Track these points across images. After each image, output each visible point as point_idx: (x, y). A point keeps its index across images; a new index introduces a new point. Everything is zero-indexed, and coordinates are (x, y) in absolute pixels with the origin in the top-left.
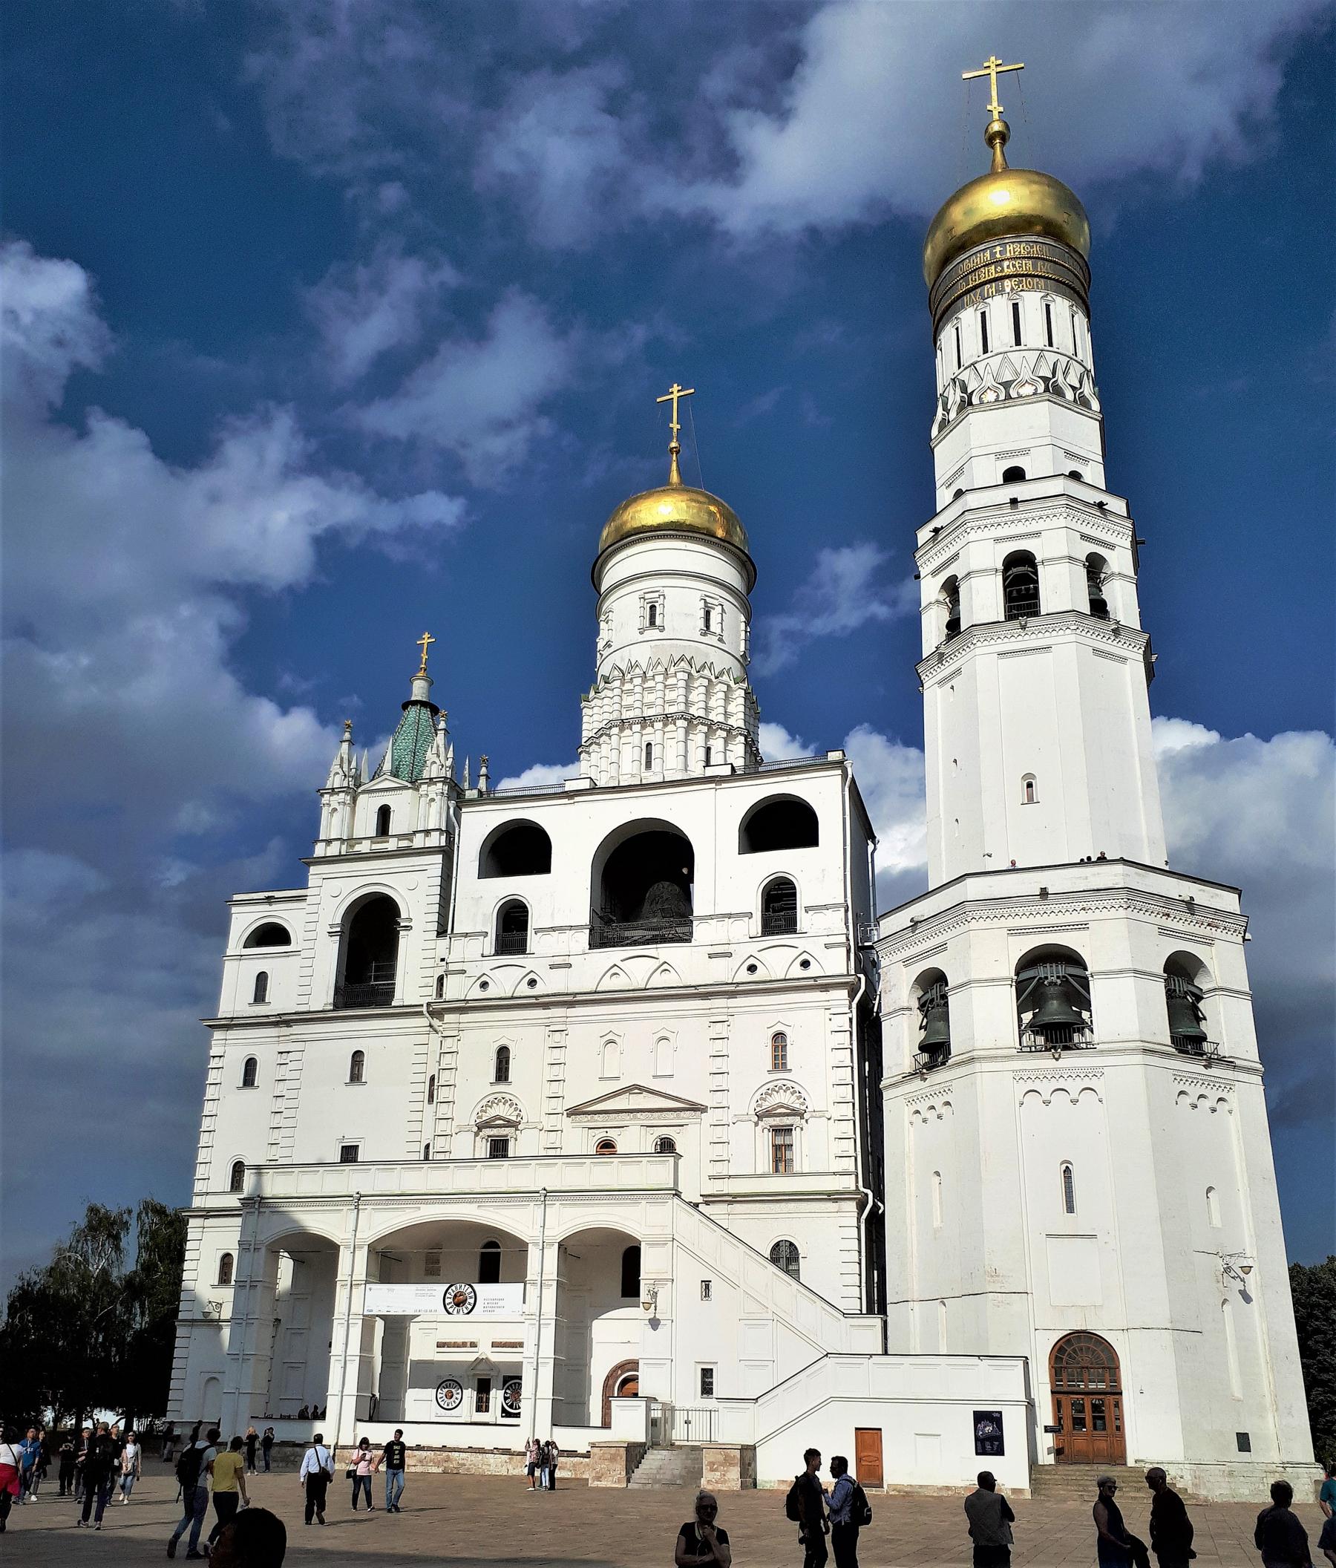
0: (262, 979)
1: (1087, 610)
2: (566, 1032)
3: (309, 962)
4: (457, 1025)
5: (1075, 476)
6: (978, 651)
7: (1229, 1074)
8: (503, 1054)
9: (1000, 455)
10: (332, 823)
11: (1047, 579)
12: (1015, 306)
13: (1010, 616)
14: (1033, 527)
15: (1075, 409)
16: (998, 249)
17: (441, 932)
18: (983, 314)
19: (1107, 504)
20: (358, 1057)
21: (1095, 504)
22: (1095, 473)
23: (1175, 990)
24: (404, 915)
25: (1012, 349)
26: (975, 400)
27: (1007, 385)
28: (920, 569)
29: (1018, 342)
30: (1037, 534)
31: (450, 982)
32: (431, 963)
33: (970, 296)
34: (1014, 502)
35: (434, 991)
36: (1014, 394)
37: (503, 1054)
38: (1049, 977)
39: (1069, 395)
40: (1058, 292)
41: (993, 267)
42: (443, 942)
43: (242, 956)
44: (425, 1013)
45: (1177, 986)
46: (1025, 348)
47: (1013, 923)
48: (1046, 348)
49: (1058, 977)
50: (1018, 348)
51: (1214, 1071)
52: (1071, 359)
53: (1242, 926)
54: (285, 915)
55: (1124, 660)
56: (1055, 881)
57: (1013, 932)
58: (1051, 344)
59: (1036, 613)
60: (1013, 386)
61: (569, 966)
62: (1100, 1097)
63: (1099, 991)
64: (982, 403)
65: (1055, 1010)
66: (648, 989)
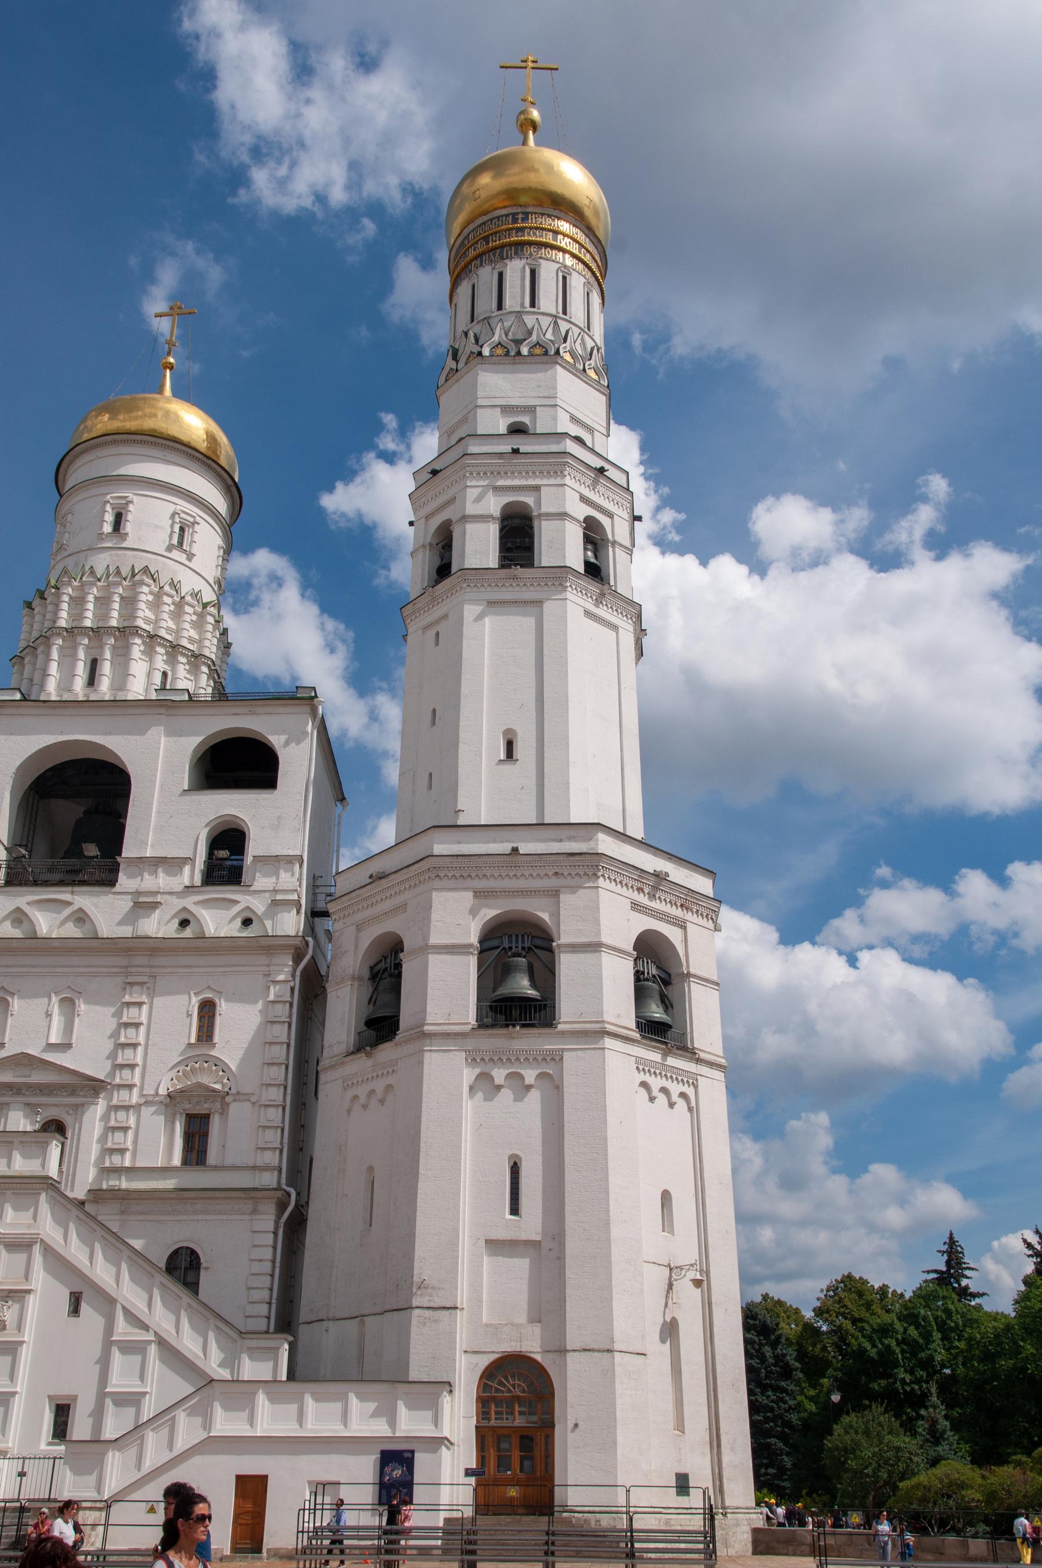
1: (581, 569)
5: (579, 440)
9: (506, 409)
11: (545, 533)
13: (502, 566)
16: (520, 216)
21: (596, 469)
23: (643, 973)
26: (486, 352)
29: (533, 304)
33: (489, 256)
34: (516, 451)
36: (525, 351)
38: (514, 947)
47: (479, 884)
50: (532, 310)
52: (584, 331)
55: (615, 628)
58: (565, 312)
62: (557, 1082)
63: (567, 966)
64: (491, 355)
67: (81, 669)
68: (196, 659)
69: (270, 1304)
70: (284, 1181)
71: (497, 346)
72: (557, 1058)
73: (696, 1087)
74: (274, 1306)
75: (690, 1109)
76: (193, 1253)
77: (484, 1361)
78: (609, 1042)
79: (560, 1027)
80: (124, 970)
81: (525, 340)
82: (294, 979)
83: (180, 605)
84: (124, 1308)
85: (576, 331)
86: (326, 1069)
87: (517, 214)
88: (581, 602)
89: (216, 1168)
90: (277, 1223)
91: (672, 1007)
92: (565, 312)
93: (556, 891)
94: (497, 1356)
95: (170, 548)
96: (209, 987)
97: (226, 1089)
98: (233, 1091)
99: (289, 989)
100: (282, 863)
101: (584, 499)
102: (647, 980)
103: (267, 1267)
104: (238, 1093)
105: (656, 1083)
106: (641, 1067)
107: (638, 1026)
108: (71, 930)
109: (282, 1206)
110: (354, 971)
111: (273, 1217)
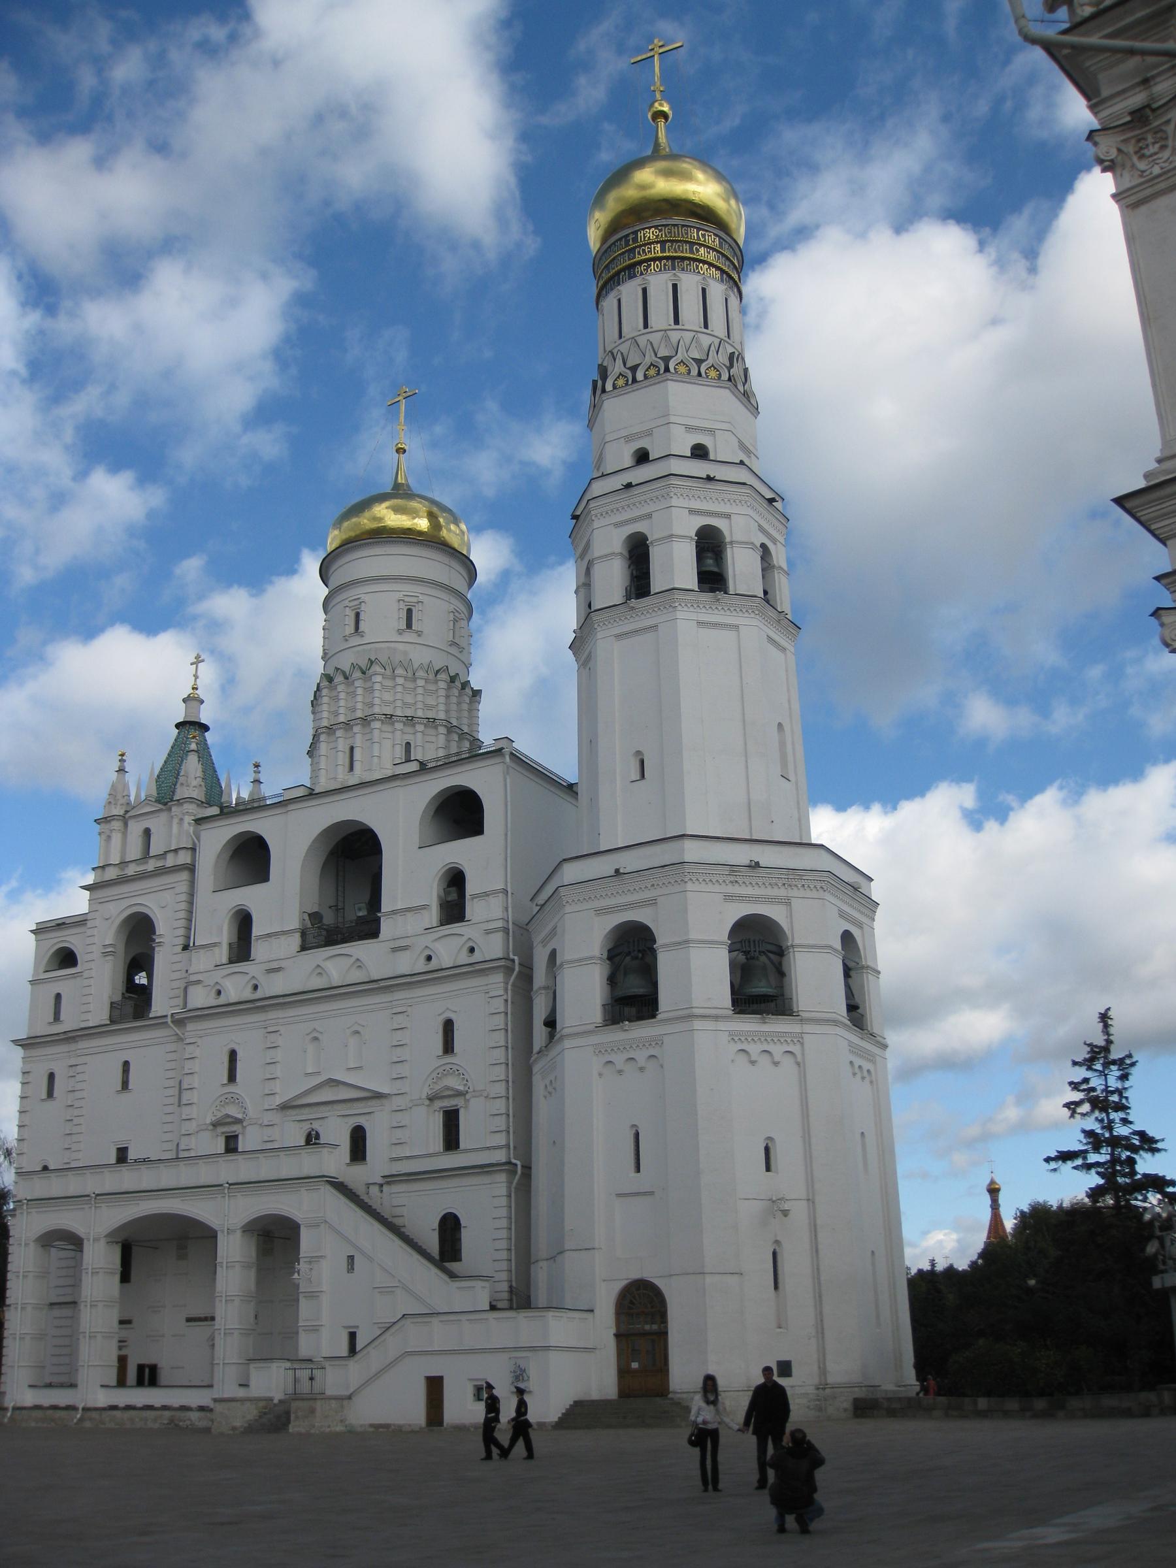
2: (279, 1033)
3: (86, 982)
6: (599, 635)
8: (233, 1055)
9: (629, 439)
12: (645, 291)
15: (700, 382)
16: (631, 237)
17: (186, 948)
18: (619, 300)
19: (715, 477)
20: (126, 1064)
25: (640, 333)
26: (609, 387)
29: (646, 326)
31: (191, 989)
32: (177, 975)
34: (629, 486)
35: (180, 1001)
36: (640, 376)
37: (233, 1055)
41: (627, 254)
42: (186, 954)
44: (170, 1023)
45: (752, 947)
48: (670, 327)
49: (639, 951)
50: (647, 330)
51: (778, 1025)
54: (73, 940)
56: (629, 862)
57: (600, 912)
58: (677, 321)
60: (639, 369)
61: (278, 970)
63: (665, 964)
65: (634, 985)
67: (343, 759)
68: (431, 722)
69: (509, 1250)
70: (512, 1156)
71: (618, 377)
72: (660, 1043)
73: (802, 1044)
74: (513, 1252)
75: (798, 1064)
77: (618, 1286)
78: (698, 1024)
79: (659, 1017)
80: (389, 1004)
82: (507, 993)
83: (414, 679)
84: (380, 1265)
85: (691, 335)
86: (535, 1060)
87: (627, 235)
89: (467, 1151)
90: (509, 1188)
91: (785, 975)
92: (677, 321)
93: (655, 900)
94: (625, 1282)
95: (400, 632)
96: (448, 1009)
97: (467, 1089)
98: (471, 1090)
100: (490, 896)
101: (692, 512)
102: (753, 958)
103: (504, 1223)
104: (474, 1091)
105: (754, 1049)
106: (736, 1039)
107: (735, 1002)
108: (356, 976)
111: (505, 1185)
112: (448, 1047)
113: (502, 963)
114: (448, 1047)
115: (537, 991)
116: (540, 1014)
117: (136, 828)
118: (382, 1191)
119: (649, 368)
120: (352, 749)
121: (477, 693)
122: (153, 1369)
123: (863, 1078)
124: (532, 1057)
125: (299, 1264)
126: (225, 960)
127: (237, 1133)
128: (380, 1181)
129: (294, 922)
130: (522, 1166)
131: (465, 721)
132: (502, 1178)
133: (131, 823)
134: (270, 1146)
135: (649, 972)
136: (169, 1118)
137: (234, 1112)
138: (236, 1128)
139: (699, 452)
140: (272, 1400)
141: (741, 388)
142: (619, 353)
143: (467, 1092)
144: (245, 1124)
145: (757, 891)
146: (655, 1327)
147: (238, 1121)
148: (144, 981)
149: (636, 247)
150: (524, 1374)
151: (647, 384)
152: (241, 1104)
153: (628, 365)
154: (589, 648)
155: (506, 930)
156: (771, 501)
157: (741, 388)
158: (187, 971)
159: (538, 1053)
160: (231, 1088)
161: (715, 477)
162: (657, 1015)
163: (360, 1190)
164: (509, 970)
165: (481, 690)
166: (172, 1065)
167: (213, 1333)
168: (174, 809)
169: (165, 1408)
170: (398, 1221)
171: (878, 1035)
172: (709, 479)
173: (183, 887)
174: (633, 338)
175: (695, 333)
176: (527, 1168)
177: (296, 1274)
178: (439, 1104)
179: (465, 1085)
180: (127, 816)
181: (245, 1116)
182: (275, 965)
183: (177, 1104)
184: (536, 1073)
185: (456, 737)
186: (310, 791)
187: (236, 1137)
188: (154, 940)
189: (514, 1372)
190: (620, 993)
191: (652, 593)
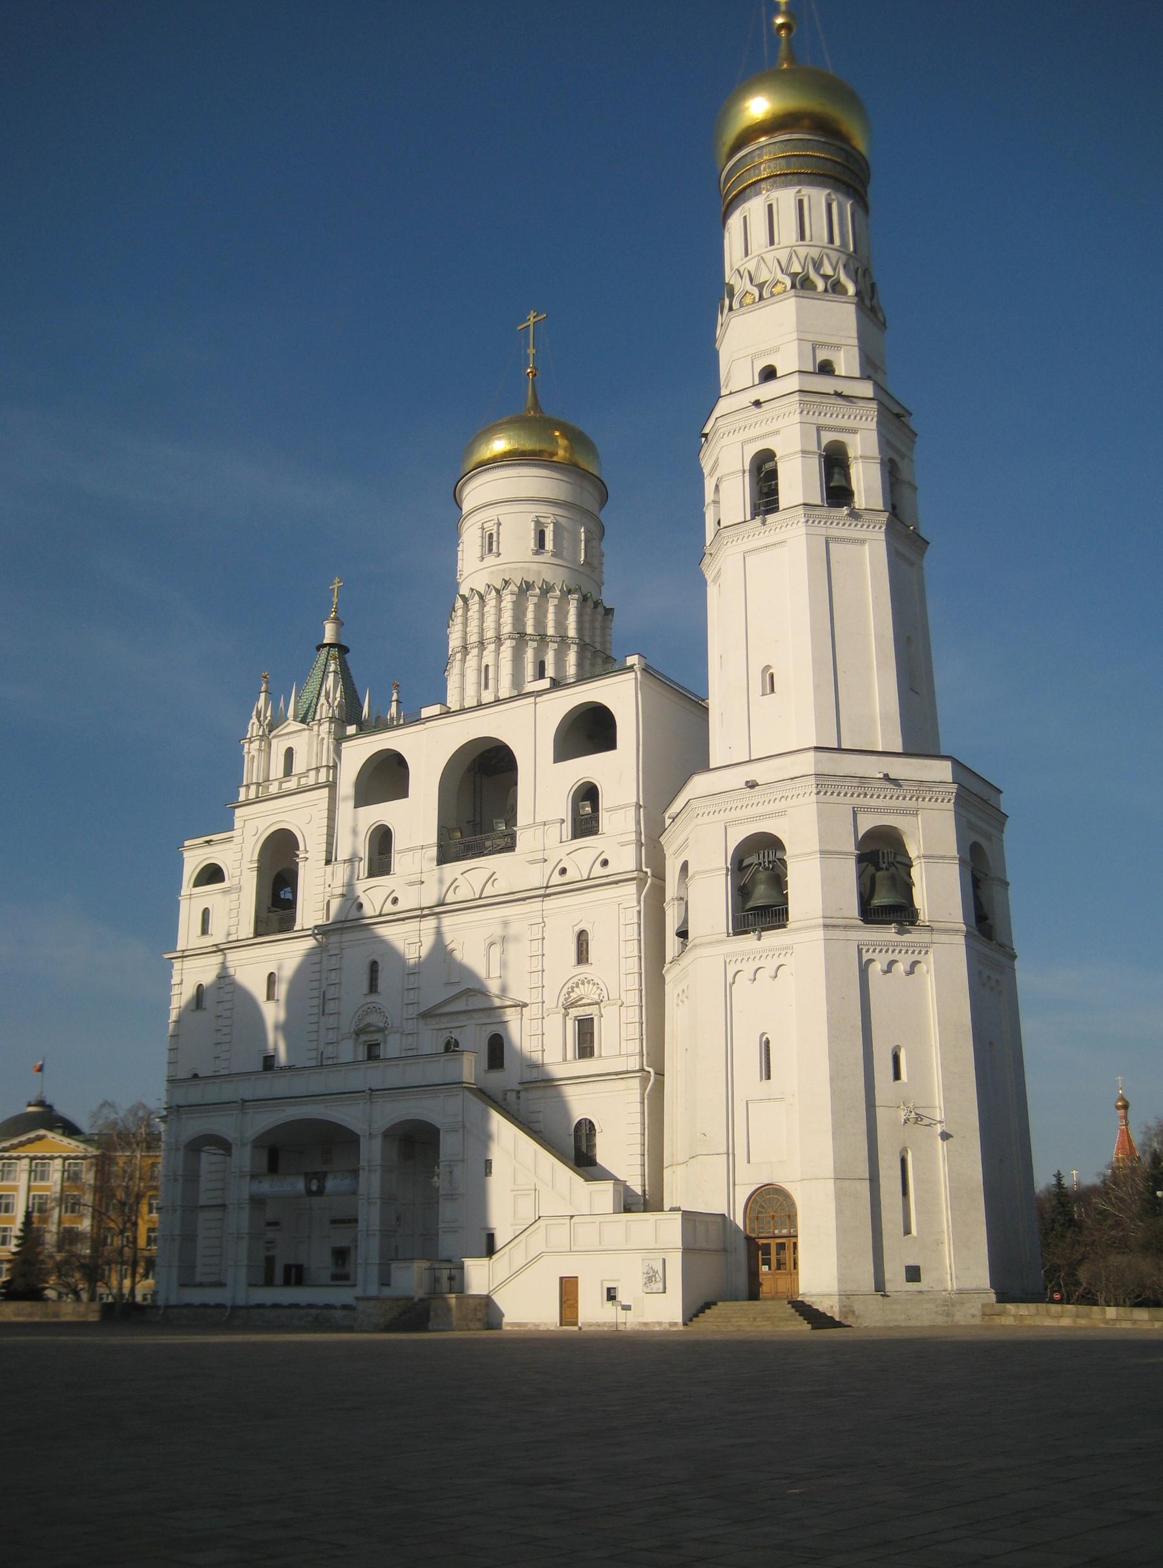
0: (206, 913)
4: (338, 945)
7: (924, 937)
10: (252, 772)
12: (770, 207)
13: (754, 516)
14: (774, 426)
18: (745, 218)
19: (842, 392)
22: (847, 362)
24: (302, 847)
25: (766, 250)
26: (735, 305)
27: (761, 286)
28: (704, 471)
29: (772, 242)
30: (777, 432)
36: (765, 294)
39: (821, 285)
40: (811, 184)
41: (752, 171)
42: (329, 868)
43: (191, 895)
46: (779, 246)
50: (773, 247)
53: (952, 793)
59: (775, 509)
64: (741, 306)
65: (761, 895)
66: (550, 887)
74: (646, 1157)
76: (590, 1122)
81: (768, 281)
88: (823, 531)
93: (785, 811)
98: (606, 998)
99: (636, 914)
109: (645, 1080)
110: (674, 893)
111: (639, 1091)
112: (582, 956)
113: (635, 874)
114: (582, 956)
115: (669, 903)
116: (672, 925)
117: (278, 748)
118: (519, 1098)
119: (776, 284)
120: (487, 666)
121: (609, 612)
122: (300, 1269)
123: (992, 989)
124: (664, 967)
125: (438, 1168)
126: (366, 875)
127: (378, 1042)
128: (518, 1087)
129: (433, 838)
130: (656, 1073)
131: (598, 639)
132: (636, 1083)
133: (274, 742)
134: (410, 1053)
135: (778, 881)
136: (315, 1027)
137: (374, 1019)
138: (378, 1037)
139: (826, 369)
140: (413, 1299)
141: (868, 302)
142: (746, 270)
143: (602, 1001)
144: (386, 1032)
145: (887, 803)
146: (785, 1231)
147: (381, 1030)
148: (289, 896)
149: (761, 163)
150: (657, 1275)
151: (774, 301)
152: (383, 1014)
153: (756, 282)
154: (718, 565)
155: (639, 845)
156: (898, 416)
157: (868, 302)
158: (329, 886)
159: (671, 963)
160: (373, 998)
161: (842, 392)
162: (787, 924)
163: (499, 1097)
164: (641, 882)
165: (613, 609)
166: (317, 976)
167: (357, 1235)
168: (316, 728)
169: (310, 1306)
170: (536, 1126)
171: (1007, 946)
172: (838, 395)
173: (325, 804)
174: (759, 255)
175: (821, 249)
176: (660, 1074)
177: (436, 1178)
178: (573, 1012)
179: (599, 995)
180: (270, 737)
181: (386, 1025)
182: (414, 878)
183: (321, 1014)
184: (669, 983)
185: (589, 655)
186: (448, 709)
187: (379, 1044)
188: (298, 856)
189: (647, 1273)
190: (751, 904)
191: (780, 509)
